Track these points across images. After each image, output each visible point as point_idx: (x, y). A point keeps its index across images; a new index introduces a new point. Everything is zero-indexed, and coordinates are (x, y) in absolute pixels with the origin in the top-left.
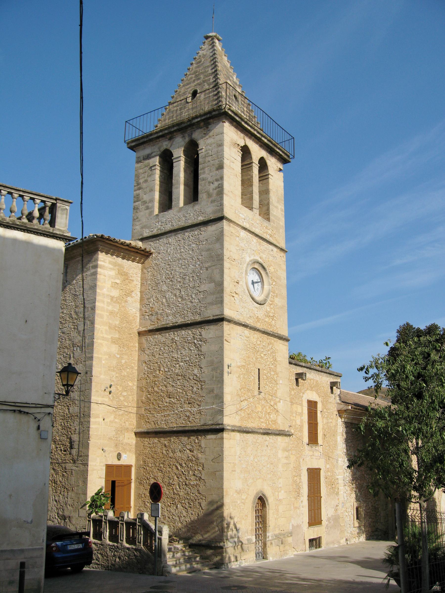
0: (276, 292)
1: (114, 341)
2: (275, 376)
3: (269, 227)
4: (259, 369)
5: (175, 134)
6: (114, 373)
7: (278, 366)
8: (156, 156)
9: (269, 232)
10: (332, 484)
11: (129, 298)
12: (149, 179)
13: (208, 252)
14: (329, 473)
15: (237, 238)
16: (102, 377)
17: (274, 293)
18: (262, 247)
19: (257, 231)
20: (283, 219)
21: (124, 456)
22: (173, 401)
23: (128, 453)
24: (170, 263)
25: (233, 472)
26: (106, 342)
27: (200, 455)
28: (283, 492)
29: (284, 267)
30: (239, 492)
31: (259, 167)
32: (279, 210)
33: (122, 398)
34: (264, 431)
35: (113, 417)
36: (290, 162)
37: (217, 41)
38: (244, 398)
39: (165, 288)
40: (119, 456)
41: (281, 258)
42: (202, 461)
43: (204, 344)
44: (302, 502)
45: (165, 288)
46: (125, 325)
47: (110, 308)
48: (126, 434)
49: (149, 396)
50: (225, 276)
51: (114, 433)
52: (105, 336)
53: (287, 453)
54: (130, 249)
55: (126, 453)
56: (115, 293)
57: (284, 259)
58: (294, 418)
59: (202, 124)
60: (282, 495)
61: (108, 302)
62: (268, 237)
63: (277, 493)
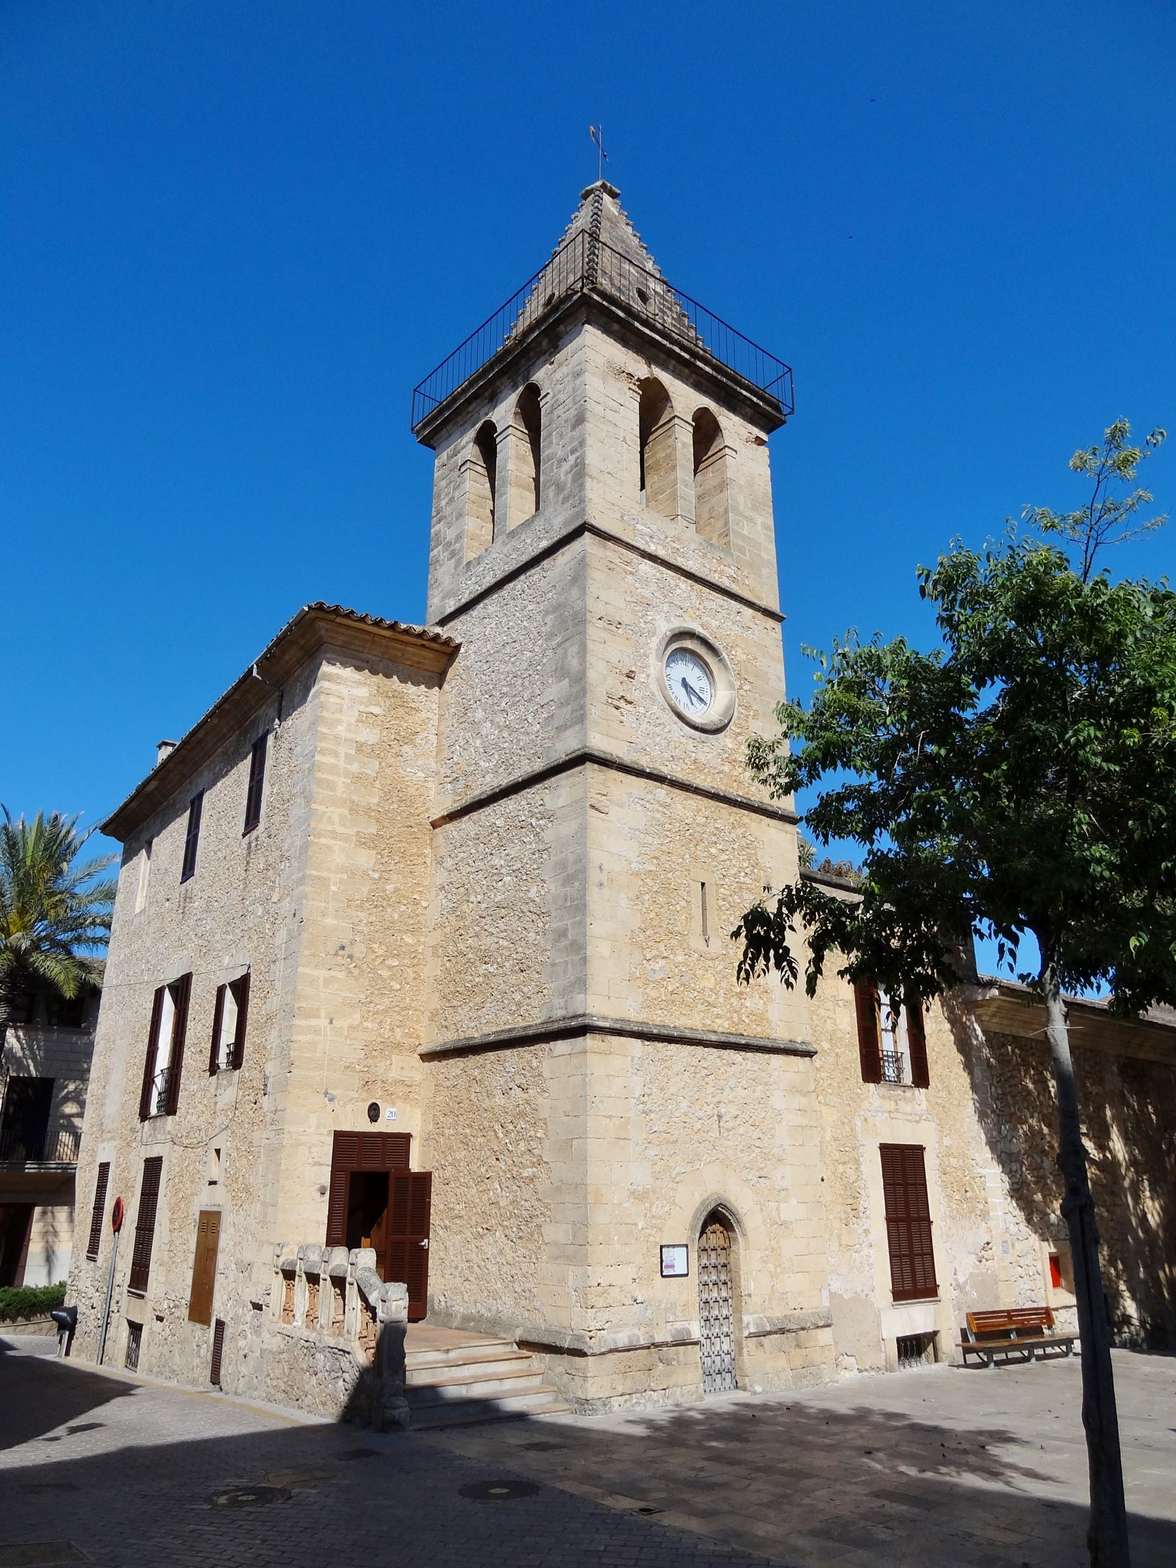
1: (363, 842)
3: (729, 560)
4: (703, 884)
5: (498, 383)
6: (362, 915)
9: (730, 571)
11: (406, 749)
12: (457, 494)
14: (953, 1161)
15: (630, 577)
16: (330, 921)
17: (747, 708)
18: (706, 603)
19: (691, 566)
20: (773, 547)
21: (385, 1111)
22: (491, 970)
23: (399, 1103)
24: (489, 658)
25: (622, 1143)
26: (340, 843)
27: (540, 1100)
28: (794, 1202)
29: (780, 654)
30: (639, 1196)
31: (694, 428)
32: (759, 527)
33: (385, 973)
35: (357, 1016)
36: (784, 422)
37: (606, 197)
38: (655, 952)
39: (480, 715)
40: (374, 1112)
41: (773, 633)
42: (545, 1114)
43: (550, 825)
45: (480, 715)
46: (395, 806)
47: (355, 768)
49: (448, 964)
50: (590, 658)
53: (804, 1100)
55: (393, 1104)
56: (369, 735)
58: (831, 1014)
59: (545, 343)
60: (790, 1210)
61: (347, 755)
62: (725, 583)
63: (772, 1205)
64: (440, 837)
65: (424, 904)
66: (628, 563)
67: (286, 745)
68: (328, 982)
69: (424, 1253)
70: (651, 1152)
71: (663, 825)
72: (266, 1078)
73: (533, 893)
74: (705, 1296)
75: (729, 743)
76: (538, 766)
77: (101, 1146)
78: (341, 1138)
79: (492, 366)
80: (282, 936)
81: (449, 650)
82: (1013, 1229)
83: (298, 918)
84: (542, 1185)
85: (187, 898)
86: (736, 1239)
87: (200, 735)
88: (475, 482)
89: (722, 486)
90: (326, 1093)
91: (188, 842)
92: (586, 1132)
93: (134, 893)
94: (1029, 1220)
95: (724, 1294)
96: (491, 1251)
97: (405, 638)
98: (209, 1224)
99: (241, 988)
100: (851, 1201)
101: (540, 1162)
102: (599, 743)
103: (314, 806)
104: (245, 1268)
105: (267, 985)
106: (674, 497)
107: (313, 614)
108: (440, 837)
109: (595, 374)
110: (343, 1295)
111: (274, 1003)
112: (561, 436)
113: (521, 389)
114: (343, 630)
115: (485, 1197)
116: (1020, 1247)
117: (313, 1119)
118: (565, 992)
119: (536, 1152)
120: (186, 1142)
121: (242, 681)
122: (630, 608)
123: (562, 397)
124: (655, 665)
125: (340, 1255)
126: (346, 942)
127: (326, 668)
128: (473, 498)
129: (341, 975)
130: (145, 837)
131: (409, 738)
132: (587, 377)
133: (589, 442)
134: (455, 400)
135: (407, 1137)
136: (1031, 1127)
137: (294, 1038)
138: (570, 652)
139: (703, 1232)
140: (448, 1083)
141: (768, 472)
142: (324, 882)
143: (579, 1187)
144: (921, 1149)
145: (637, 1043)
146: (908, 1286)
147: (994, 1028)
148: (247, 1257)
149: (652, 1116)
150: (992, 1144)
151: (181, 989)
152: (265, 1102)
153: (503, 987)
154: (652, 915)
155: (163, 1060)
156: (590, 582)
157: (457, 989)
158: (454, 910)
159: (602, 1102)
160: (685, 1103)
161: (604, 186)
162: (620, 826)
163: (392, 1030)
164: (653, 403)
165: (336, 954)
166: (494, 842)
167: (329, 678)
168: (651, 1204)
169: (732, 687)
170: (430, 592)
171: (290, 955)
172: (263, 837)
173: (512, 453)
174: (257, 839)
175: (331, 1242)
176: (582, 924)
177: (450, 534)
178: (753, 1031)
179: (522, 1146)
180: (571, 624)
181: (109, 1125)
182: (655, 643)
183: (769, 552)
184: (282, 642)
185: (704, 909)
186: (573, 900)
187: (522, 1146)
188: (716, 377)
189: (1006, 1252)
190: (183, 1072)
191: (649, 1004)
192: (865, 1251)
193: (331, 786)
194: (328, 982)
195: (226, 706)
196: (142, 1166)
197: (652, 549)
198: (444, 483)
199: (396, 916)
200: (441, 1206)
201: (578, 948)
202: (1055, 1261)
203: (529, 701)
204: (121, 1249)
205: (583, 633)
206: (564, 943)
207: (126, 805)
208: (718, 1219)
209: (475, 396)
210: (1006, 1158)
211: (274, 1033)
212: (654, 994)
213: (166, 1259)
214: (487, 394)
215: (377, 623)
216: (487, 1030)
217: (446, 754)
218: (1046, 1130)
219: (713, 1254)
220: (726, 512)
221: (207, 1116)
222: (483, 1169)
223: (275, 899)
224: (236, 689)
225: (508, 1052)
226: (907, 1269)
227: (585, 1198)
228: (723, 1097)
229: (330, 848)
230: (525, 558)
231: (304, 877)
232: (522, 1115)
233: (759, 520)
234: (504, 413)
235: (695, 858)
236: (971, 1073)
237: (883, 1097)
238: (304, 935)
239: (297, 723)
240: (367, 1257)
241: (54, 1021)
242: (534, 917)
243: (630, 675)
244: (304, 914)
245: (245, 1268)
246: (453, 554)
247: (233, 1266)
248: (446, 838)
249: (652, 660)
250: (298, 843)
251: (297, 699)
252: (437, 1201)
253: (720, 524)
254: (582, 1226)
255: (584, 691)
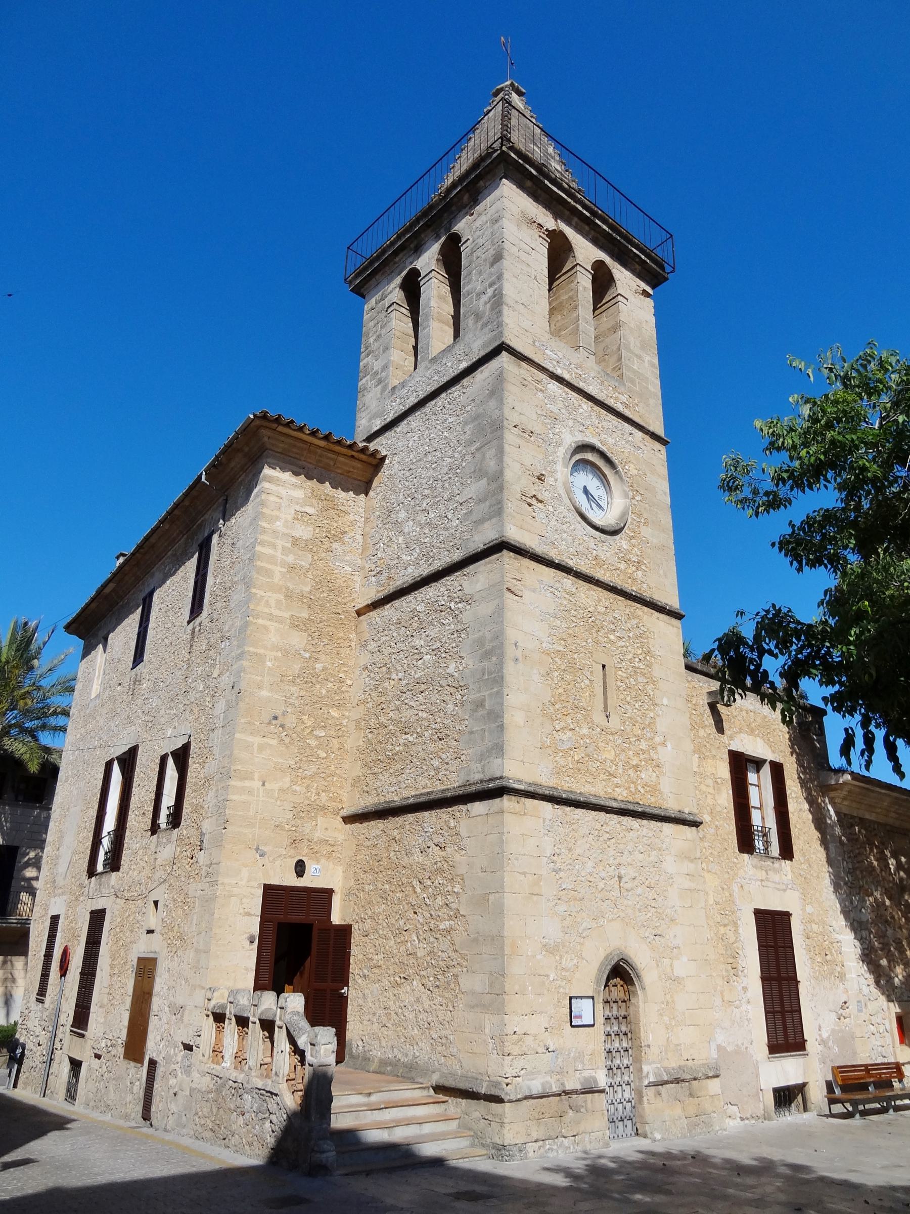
0: (645, 516)
1: (297, 625)
2: (649, 688)
3: (622, 389)
4: (604, 666)
6: (294, 689)
7: (656, 667)
8: (394, 289)
9: (624, 398)
10: (825, 954)
11: (335, 545)
12: (384, 331)
13: (476, 423)
14: (815, 927)
15: (540, 394)
16: (265, 693)
17: (639, 515)
18: (604, 423)
19: (591, 390)
20: (658, 382)
22: (411, 739)
23: (323, 861)
25: (535, 898)
27: (457, 857)
28: (685, 959)
29: (664, 471)
30: (551, 949)
32: (646, 364)
34: (623, 806)
36: (666, 279)
38: (563, 724)
40: (300, 868)
41: (657, 455)
43: (468, 607)
44: (745, 989)
45: (402, 515)
46: (325, 595)
47: (290, 559)
48: (320, 820)
49: (370, 736)
50: (507, 460)
51: (290, 815)
52: (276, 612)
54: (332, 447)
55: (318, 862)
56: (304, 532)
57: (664, 457)
59: (466, 198)
60: (682, 967)
62: (620, 408)
64: (365, 623)
65: (349, 682)
66: (539, 382)
67: (230, 541)
68: (261, 748)
69: (344, 1000)
70: (562, 908)
71: (569, 611)
72: (202, 834)
73: (451, 669)
74: (608, 1046)
75: (625, 545)
76: (457, 556)
77: (53, 900)
78: (270, 892)
79: (418, 220)
80: (221, 706)
81: (374, 462)
82: (866, 990)
83: (236, 690)
84: (459, 937)
85: (137, 681)
86: (635, 993)
87: (152, 540)
88: (400, 322)
89: (616, 328)
90: (257, 849)
91: (139, 634)
92: (502, 887)
93: (90, 681)
94: (877, 983)
95: (625, 1045)
96: (408, 999)
97: (337, 448)
98: (146, 969)
99: (182, 756)
100: (731, 961)
101: (457, 915)
102: (514, 534)
103: (253, 590)
104: (178, 1010)
105: (206, 751)
106: (576, 331)
107: (258, 422)
108: (365, 623)
109: (510, 222)
110: (271, 1038)
111: (211, 767)
112: (480, 273)
113: (443, 239)
114: (282, 439)
115: (403, 948)
116: (872, 1007)
117: (245, 873)
118: (482, 758)
119: (453, 906)
120: (127, 895)
121: (192, 488)
122: (540, 423)
123: (481, 241)
124: (561, 470)
125: (268, 999)
126: (279, 713)
127: (267, 471)
128: (398, 334)
129: (274, 742)
130: (101, 634)
131: (339, 536)
132: (505, 222)
133: (506, 276)
134: (384, 251)
135: (329, 892)
136: (876, 899)
137: (231, 797)
138: (487, 456)
139: (606, 985)
140: (368, 843)
141: (653, 319)
142: (261, 658)
143: (497, 939)
144: (787, 915)
145: (548, 806)
146: (781, 1040)
147: (845, 810)
148: (180, 1001)
149: (562, 874)
150: (846, 913)
151: (128, 761)
152: (201, 857)
153: (422, 754)
154: (560, 690)
155: (110, 824)
156: (506, 394)
157: (377, 758)
158: (376, 687)
159: (517, 859)
160: (590, 864)
161: (512, 85)
162: (533, 608)
163: (318, 794)
164: (559, 254)
165: (270, 723)
166: (415, 625)
167: (270, 480)
168: (561, 957)
169: (626, 496)
170: (358, 415)
171: (229, 724)
172: (206, 622)
173: (434, 292)
174: (200, 625)
175: (259, 986)
176: (499, 695)
177: (377, 365)
178: (648, 801)
179: (440, 900)
180: (490, 431)
181: (60, 881)
182: (562, 452)
183: (655, 386)
184: (229, 450)
185: (605, 688)
186: (490, 673)
187: (440, 900)
188: (610, 235)
189: (860, 1011)
190: (128, 833)
191: (558, 771)
192: (744, 1007)
193: (268, 573)
194: (261, 748)
195: (176, 512)
196: (88, 917)
197: (559, 371)
198: (372, 323)
199: (324, 692)
200: (361, 957)
201: (496, 717)
202: (900, 1020)
203: (449, 500)
204: (66, 992)
205: (501, 438)
206: (481, 712)
207: (87, 605)
208: (620, 973)
209: (402, 248)
210: (857, 926)
211: (211, 794)
212: (562, 762)
213: (105, 1001)
214: (412, 246)
215: (314, 433)
216: (406, 793)
217: (371, 551)
218: (888, 902)
219: (615, 1006)
220: (619, 349)
221: (147, 872)
222: (401, 922)
223: (215, 675)
224: (186, 495)
225: (426, 814)
226: (780, 1026)
227: (502, 949)
228: (624, 859)
229: (266, 628)
230: (446, 379)
231: (243, 653)
232: (440, 871)
233: (647, 358)
234: (428, 260)
235: (597, 643)
236: (826, 849)
237: (755, 867)
238: (242, 705)
239: (240, 522)
240: (295, 1002)
241: (21, 798)
242: (452, 690)
243: (541, 478)
244: (243, 685)
245: (178, 1010)
246: (380, 382)
247: (167, 1009)
248: (370, 624)
249: (559, 467)
250: (238, 623)
251: (240, 501)
252: (356, 952)
253: (615, 357)
254: (499, 976)
255: (501, 488)
